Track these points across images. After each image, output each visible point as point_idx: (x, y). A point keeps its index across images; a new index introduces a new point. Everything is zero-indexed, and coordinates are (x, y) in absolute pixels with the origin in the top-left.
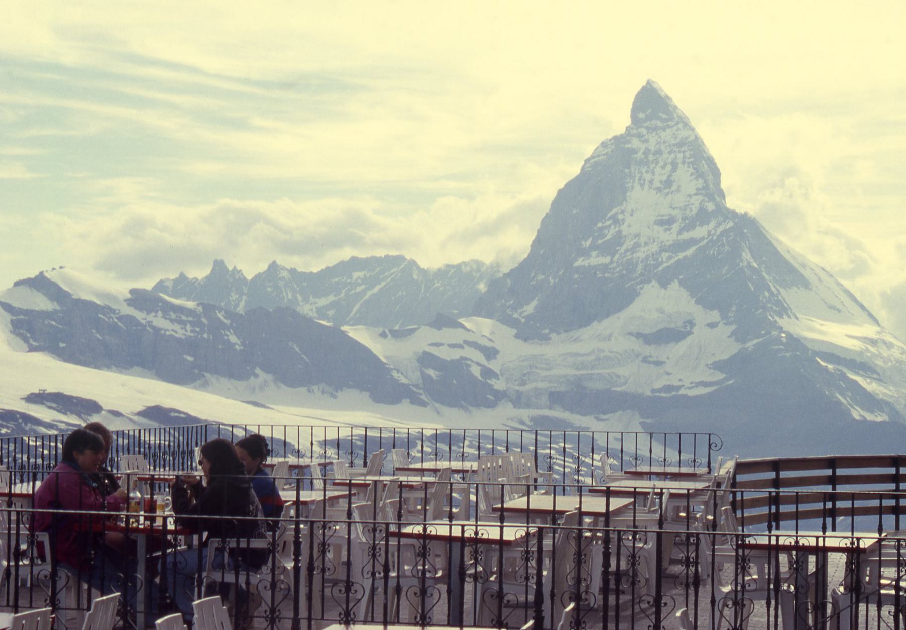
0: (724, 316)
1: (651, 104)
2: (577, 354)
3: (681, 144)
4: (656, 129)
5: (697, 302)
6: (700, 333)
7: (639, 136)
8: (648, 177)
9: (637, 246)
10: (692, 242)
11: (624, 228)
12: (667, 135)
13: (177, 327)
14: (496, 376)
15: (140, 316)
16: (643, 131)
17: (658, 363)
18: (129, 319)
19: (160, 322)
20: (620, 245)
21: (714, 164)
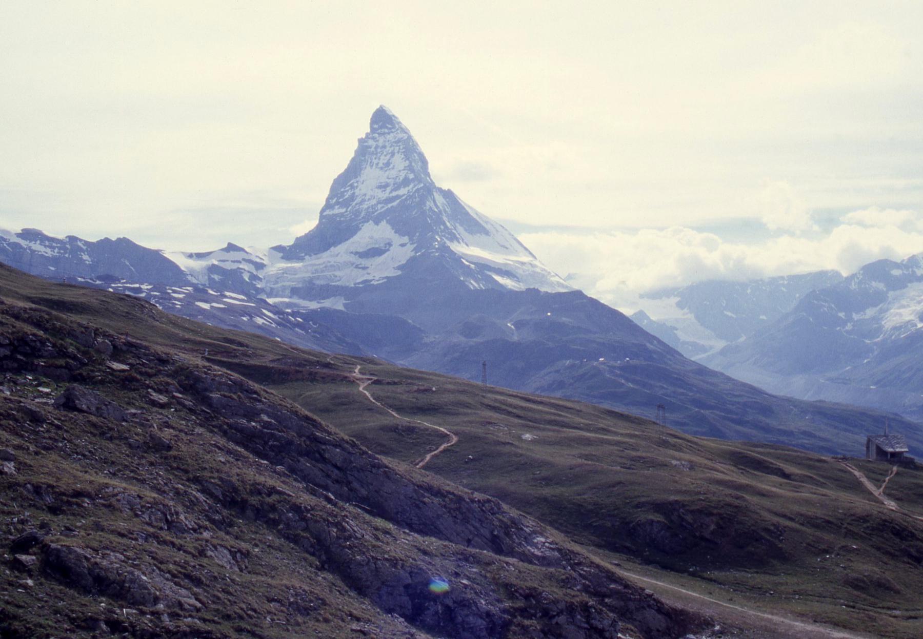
0: (411, 239)
1: (382, 120)
2: (315, 265)
3: (399, 141)
4: (384, 134)
5: (396, 232)
6: (395, 250)
7: (374, 138)
8: (375, 161)
9: (363, 201)
10: (398, 197)
11: (357, 192)
12: (390, 137)
13: (48, 250)
14: (260, 279)
15: (24, 243)
16: (376, 135)
17: (364, 268)
18: (16, 245)
19: (37, 246)
20: (353, 201)
21: (424, 158)
